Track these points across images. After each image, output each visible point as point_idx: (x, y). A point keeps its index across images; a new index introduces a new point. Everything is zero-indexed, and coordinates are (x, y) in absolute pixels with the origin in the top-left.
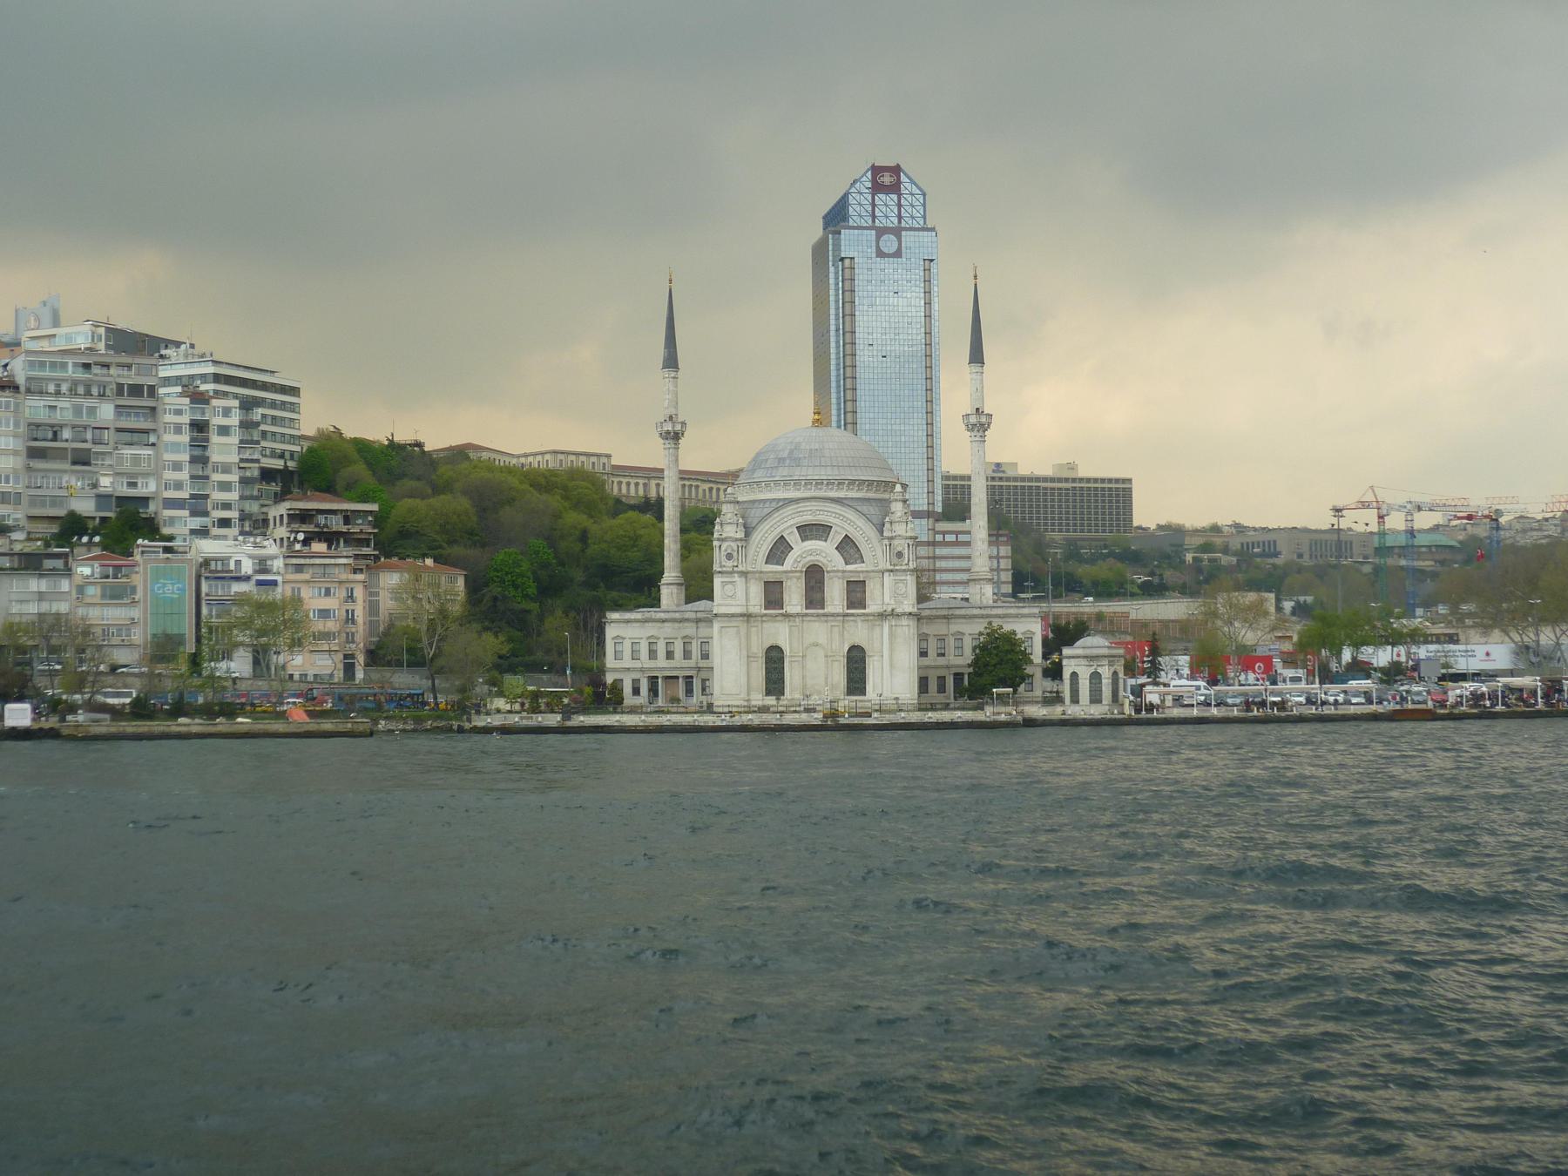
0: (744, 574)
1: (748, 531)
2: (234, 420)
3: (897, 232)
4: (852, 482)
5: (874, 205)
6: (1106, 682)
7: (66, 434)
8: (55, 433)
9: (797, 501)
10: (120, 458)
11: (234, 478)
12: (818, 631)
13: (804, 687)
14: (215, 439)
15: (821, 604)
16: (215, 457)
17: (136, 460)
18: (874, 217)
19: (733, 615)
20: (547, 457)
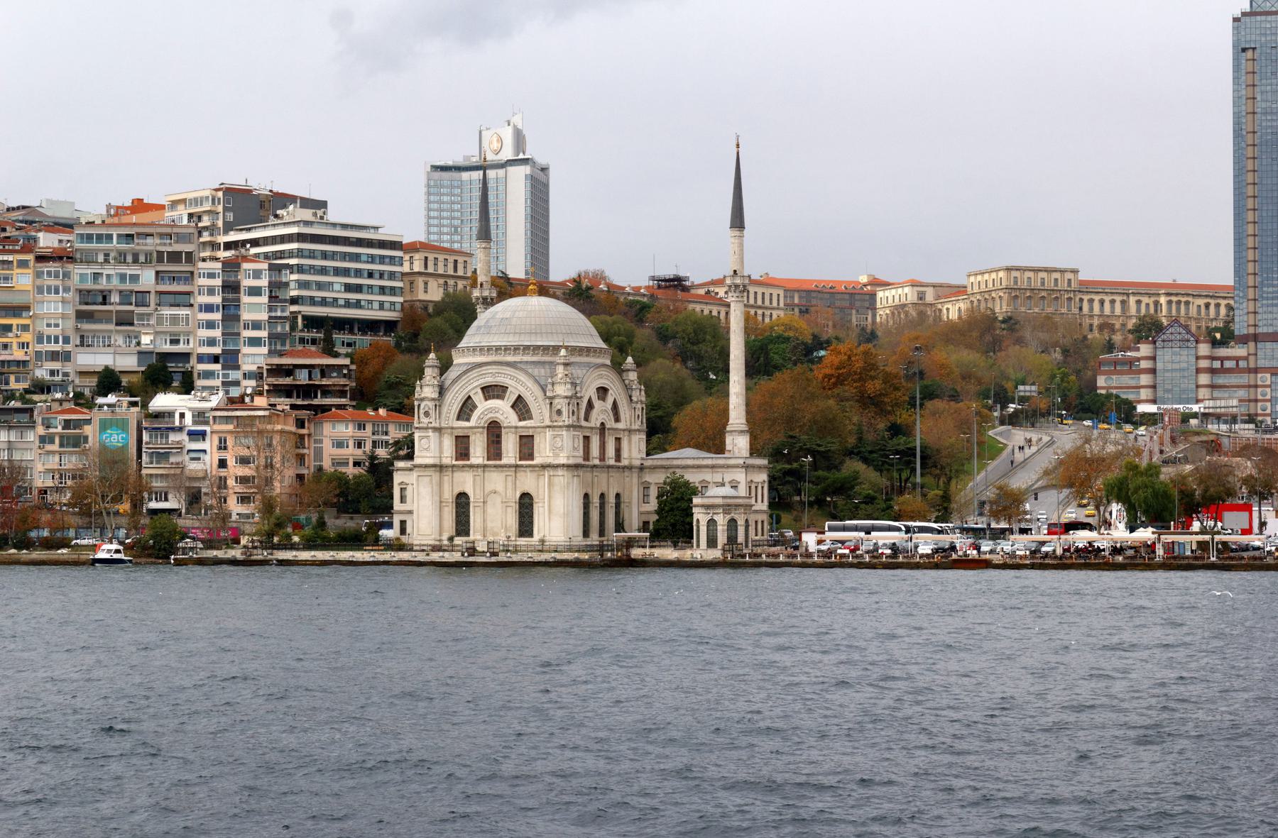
0: (439, 430)
1: (442, 391)
2: (263, 282)
4: (527, 348)
7: (115, 298)
8: (104, 298)
9: (481, 365)
10: (160, 320)
11: (263, 334)
12: (496, 480)
13: (485, 529)
14: (246, 299)
15: (498, 456)
16: (246, 316)
17: (175, 320)
19: (426, 466)
20: (1001, 274)
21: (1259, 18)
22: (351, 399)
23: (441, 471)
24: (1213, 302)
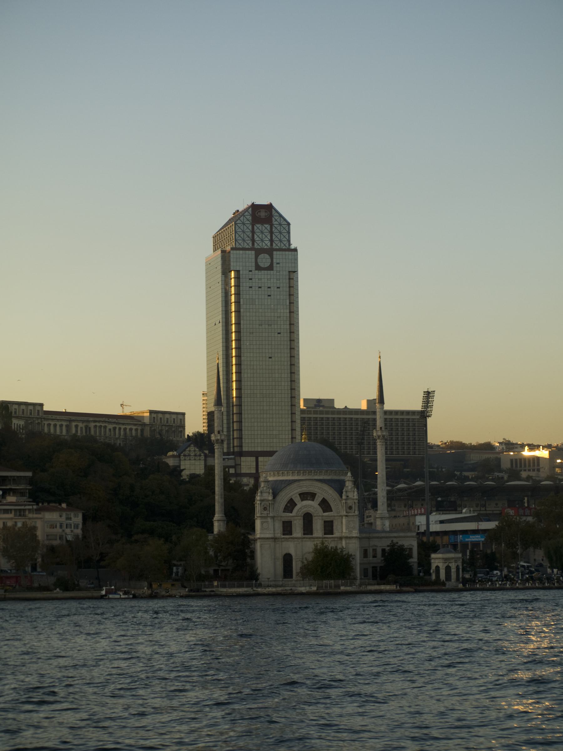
3: (270, 252)
5: (253, 232)
6: (453, 570)
18: (253, 241)
19: (268, 538)
21: (241, 252)
22: (29, 497)
23: (275, 542)
24: (117, 426)
